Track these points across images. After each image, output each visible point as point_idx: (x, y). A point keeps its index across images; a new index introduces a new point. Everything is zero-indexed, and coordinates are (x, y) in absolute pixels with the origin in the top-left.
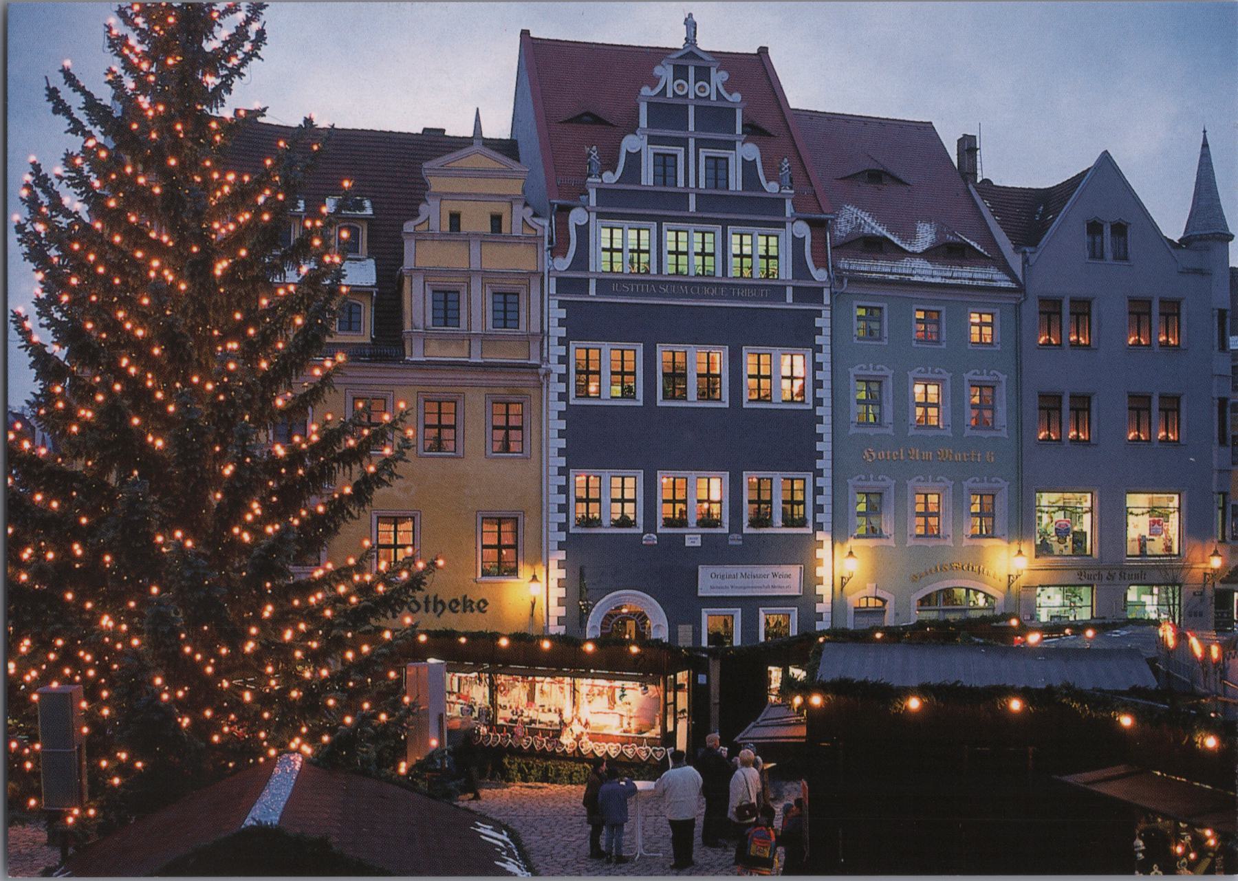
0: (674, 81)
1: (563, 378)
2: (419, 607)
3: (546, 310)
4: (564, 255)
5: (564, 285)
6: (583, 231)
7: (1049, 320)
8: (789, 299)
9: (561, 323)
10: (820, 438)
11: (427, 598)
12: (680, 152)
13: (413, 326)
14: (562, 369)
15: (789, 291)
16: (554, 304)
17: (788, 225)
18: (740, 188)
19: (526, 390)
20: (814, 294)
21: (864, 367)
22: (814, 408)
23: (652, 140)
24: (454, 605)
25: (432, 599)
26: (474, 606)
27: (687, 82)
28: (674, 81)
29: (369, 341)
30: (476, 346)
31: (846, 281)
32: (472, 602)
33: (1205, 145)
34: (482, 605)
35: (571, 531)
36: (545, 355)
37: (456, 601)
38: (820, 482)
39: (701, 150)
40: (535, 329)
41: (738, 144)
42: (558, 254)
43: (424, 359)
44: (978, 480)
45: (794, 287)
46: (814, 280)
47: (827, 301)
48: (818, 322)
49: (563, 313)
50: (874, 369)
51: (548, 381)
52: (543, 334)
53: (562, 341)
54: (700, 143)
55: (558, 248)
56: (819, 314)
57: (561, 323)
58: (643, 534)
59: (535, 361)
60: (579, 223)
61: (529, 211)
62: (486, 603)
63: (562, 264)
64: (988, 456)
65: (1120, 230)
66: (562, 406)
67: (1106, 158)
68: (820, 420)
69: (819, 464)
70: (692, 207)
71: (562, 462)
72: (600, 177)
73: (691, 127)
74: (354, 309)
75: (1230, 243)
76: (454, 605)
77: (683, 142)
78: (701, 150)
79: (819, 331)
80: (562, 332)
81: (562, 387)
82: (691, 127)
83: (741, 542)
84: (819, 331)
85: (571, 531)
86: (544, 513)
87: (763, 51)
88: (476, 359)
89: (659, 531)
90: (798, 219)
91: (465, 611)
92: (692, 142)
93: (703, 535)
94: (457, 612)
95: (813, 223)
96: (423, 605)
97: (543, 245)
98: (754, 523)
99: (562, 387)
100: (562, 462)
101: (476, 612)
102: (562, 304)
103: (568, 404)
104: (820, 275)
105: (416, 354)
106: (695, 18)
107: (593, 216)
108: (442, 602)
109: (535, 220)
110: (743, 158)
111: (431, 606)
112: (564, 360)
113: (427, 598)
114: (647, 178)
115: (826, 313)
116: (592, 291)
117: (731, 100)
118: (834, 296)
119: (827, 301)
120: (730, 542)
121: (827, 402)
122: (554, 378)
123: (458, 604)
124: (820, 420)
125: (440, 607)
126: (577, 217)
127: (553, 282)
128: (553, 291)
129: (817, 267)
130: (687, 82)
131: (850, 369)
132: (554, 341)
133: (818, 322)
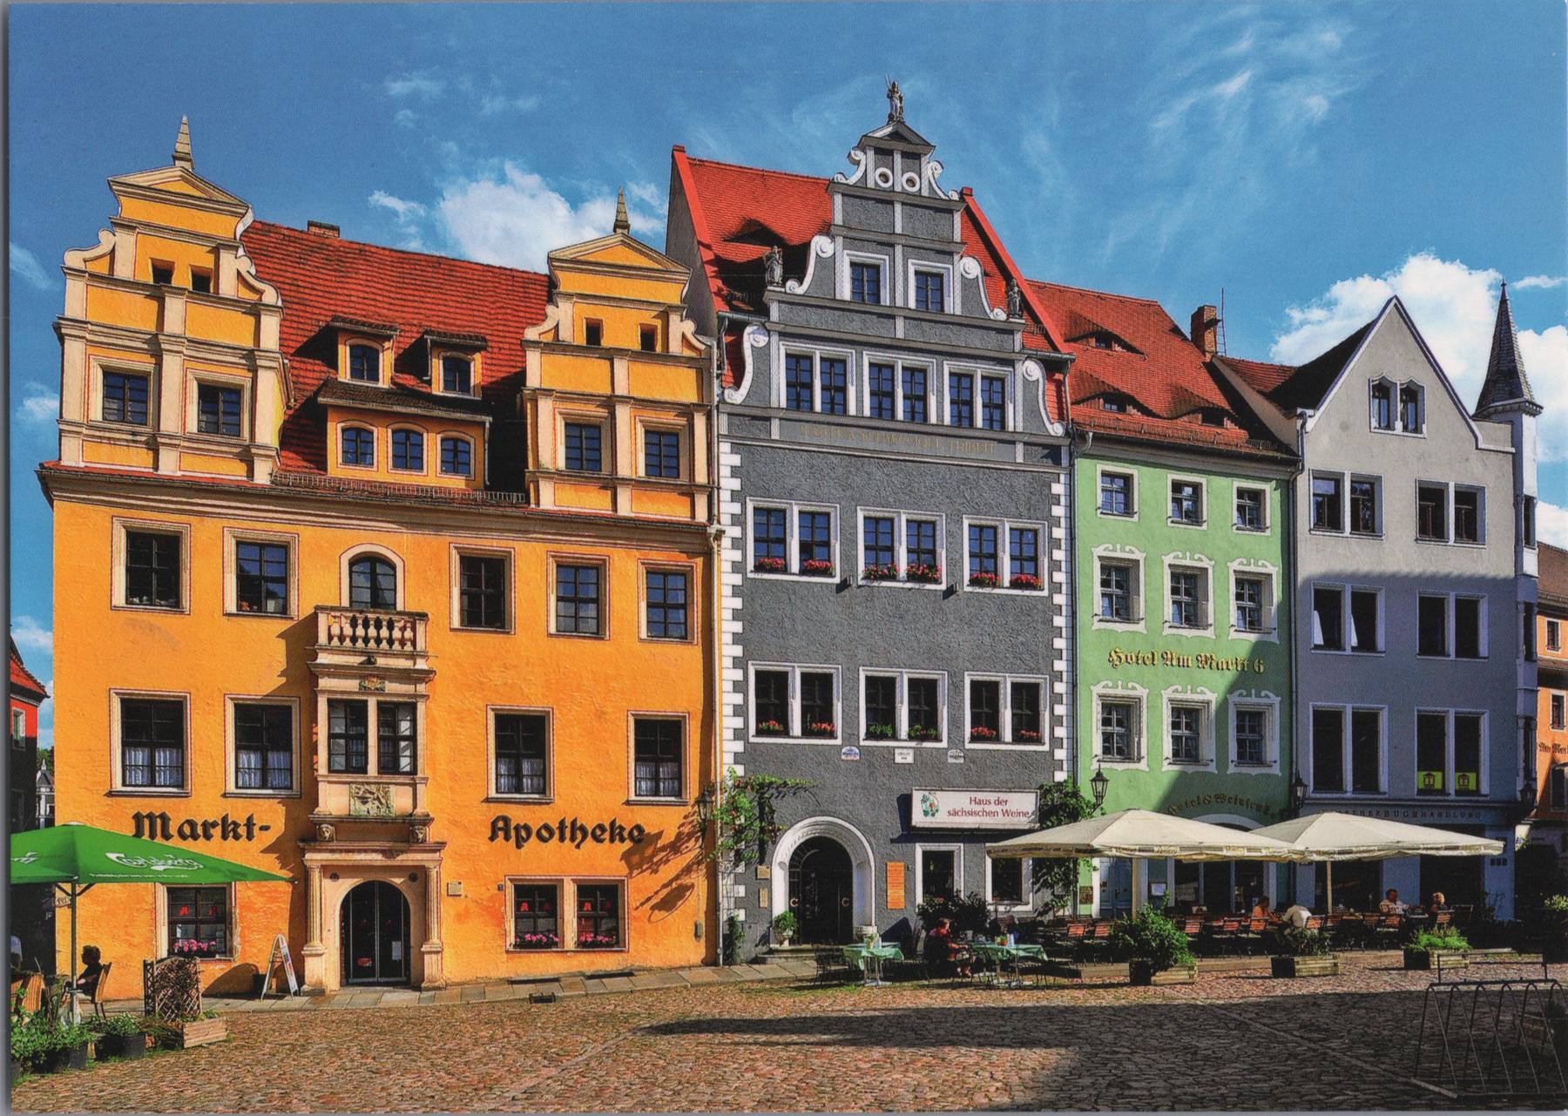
1: (738, 544)
4: (737, 384)
6: (762, 354)
9: (735, 472)
14: (736, 532)
21: (1111, 547)
43: (556, 508)
44: (1245, 693)
49: (736, 460)
50: (1123, 550)
51: (719, 546)
53: (736, 496)
57: (735, 472)
60: (756, 344)
63: (737, 397)
66: (737, 579)
71: (738, 651)
72: (784, 285)
80: (736, 484)
97: (710, 374)
100: (738, 651)
102: (735, 449)
103: (745, 578)
105: (549, 498)
107: (775, 338)
112: (738, 520)
114: (845, 291)
122: (726, 542)
126: (752, 338)
127: (724, 419)
128: (724, 431)
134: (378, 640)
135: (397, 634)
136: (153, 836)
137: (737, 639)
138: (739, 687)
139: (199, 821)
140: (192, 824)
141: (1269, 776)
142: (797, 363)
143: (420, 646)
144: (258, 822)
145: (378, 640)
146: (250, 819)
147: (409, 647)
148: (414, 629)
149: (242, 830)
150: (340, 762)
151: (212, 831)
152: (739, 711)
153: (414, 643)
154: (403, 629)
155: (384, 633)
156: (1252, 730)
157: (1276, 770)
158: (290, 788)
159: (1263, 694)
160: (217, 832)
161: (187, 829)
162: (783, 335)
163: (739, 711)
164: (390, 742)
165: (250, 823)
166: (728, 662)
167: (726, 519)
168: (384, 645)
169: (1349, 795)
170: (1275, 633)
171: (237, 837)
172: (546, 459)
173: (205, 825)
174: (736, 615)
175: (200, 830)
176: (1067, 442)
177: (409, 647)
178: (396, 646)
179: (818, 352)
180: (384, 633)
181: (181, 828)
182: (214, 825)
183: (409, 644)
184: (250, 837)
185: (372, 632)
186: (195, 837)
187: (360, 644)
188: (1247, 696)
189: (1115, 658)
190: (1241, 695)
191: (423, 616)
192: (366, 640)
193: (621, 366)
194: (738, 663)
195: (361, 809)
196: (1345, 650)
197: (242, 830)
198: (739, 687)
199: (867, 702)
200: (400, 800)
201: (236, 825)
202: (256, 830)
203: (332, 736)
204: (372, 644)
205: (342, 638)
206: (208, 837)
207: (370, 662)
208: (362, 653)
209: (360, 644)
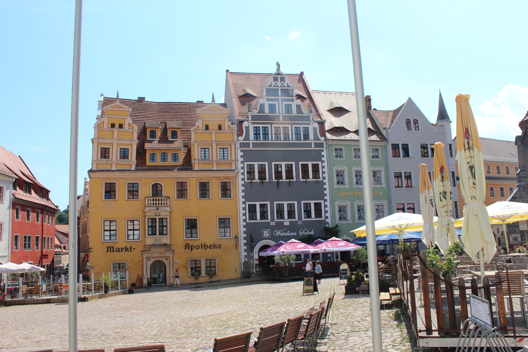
1: (243, 174)
2: (199, 247)
3: (236, 152)
5: (242, 145)
6: (247, 128)
7: (395, 150)
9: (242, 156)
10: (325, 189)
11: (202, 244)
12: (276, 103)
13: (195, 160)
14: (242, 171)
16: (239, 151)
17: (312, 124)
19: (231, 178)
20: (321, 145)
24: (210, 246)
25: (203, 245)
26: (217, 247)
29: (181, 165)
30: (215, 165)
32: (216, 245)
33: (440, 94)
34: (220, 246)
35: (248, 222)
36: (237, 167)
37: (211, 245)
39: (283, 102)
40: (233, 158)
41: (295, 100)
42: (240, 136)
48: (323, 153)
49: (242, 154)
52: (236, 160)
53: (242, 162)
55: (240, 134)
56: (323, 151)
57: (242, 156)
58: (271, 222)
59: (234, 168)
61: (230, 123)
62: (221, 246)
63: (241, 138)
64: (380, 193)
65: (416, 122)
66: (243, 182)
67: (410, 100)
68: (325, 184)
71: (244, 200)
74: (176, 155)
75: (451, 124)
76: (210, 246)
77: (277, 100)
78: (283, 102)
79: (323, 156)
80: (242, 159)
81: (243, 177)
83: (302, 224)
84: (323, 156)
85: (248, 222)
86: (238, 216)
87: (302, 73)
88: (215, 168)
89: (276, 221)
91: (214, 248)
94: (211, 248)
96: (201, 247)
99: (243, 177)
100: (244, 200)
101: (218, 248)
102: (241, 151)
103: (245, 182)
106: (279, 63)
107: (250, 123)
108: (206, 245)
109: (232, 125)
111: (203, 247)
112: (243, 168)
113: (202, 244)
115: (325, 151)
116: (251, 146)
118: (327, 145)
119: (325, 146)
120: (299, 224)
122: (240, 174)
123: (212, 246)
124: (325, 184)
125: (206, 247)
126: (245, 124)
128: (239, 146)
129: (321, 137)
130: (278, 81)
131: (333, 168)
132: (239, 162)
133: (323, 153)
134: (159, 204)
135: (163, 202)
136: (111, 251)
137: (243, 197)
138: (244, 209)
139: (120, 248)
140: (119, 248)
142: (256, 129)
143: (168, 205)
144: (133, 248)
145: (159, 204)
146: (131, 247)
147: (165, 205)
148: (167, 201)
149: (129, 250)
150: (150, 233)
151: (123, 250)
152: (244, 215)
153: (167, 204)
154: (164, 201)
155: (160, 202)
158: (139, 239)
160: (124, 250)
161: (117, 250)
162: (252, 123)
163: (244, 215)
164: (162, 227)
165: (131, 248)
166: (241, 203)
167: (240, 168)
168: (160, 205)
170: (384, 185)
171: (128, 251)
172: (196, 157)
173: (121, 248)
174: (243, 191)
175: (120, 250)
176: (325, 141)
177: (165, 205)
178: (163, 205)
179: (261, 126)
180: (160, 202)
181: (116, 250)
182: (123, 248)
183: (165, 204)
184: (131, 251)
185: (157, 202)
186: (119, 251)
187: (155, 205)
191: (169, 197)
192: (156, 204)
193: (214, 135)
194: (244, 203)
195: (156, 243)
197: (129, 250)
198: (244, 209)
200: (165, 240)
201: (128, 248)
202: (132, 249)
203: (149, 227)
204: (157, 205)
205: (151, 204)
206: (122, 251)
207: (157, 209)
208: (155, 206)
209: (155, 205)
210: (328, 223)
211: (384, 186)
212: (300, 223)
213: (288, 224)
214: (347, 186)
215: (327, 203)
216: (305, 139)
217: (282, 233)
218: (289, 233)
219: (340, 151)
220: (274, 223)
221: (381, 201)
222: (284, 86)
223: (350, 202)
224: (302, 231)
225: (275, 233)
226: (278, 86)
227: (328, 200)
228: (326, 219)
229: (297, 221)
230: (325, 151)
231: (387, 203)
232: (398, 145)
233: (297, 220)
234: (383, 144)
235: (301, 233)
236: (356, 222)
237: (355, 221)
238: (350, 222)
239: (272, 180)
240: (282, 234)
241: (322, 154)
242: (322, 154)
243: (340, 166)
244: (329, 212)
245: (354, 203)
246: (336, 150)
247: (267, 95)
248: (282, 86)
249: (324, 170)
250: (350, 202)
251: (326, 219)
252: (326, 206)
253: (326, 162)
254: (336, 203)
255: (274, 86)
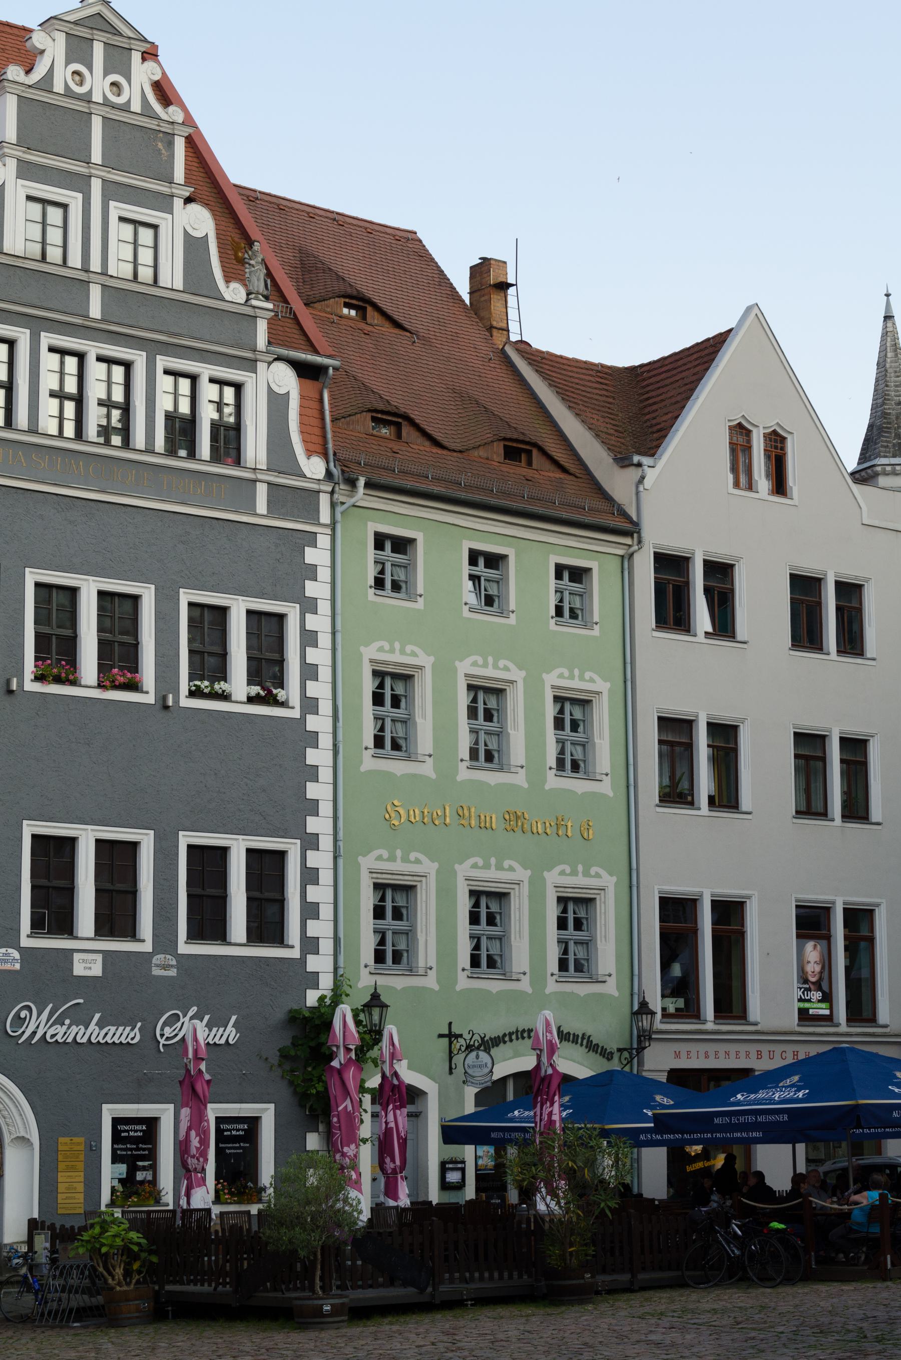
0: (67, 63)
8: (262, 506)
10: (313, 773)
12: (74, 200)
15: (262, 491)
17: (261, 366)
18: (179, 284)
22: (303, 720)
23: (26, 171)
27: (90, 69)
28: (67, 63)
31: (362, 482)
33: (888, 318)
38: (314, 859)
39: (112, 204)
41: (178, 203)
44: (568, 870)
45: (269, 484)
46: (305, 476)
47: (325, 516)
48: (311, 556)
54: (112, 191)
68: (313, 739)
69: (313, 825)
70: (95, 311)
73: (96, 156)
77: (81, 183)
78: (112, 204)
79: (312, 572)
82: (96, 156)
83: (173, 973)
84: (312, 572)
89: (25, 942)
90: (279, 359)
92: (96, 186)
93: (106, 954)
95: (305, 371)
98: (196, 933)
104: (314, 468)
110: (185, 232)
115: (324, 541)
117: (164, 116)
118: (339, 509)
119: (325, 516)
120: (156, 972)
121: (325, 707)
124: (313, 739)
129: (309, 453)
130: (90, 69)
131: (362, 649)
133: (311, 556)
141: (601, 995)
156: (578, 925)
157: (611, 988)
159: (594, 870)
169: (710, 1026)
170: (607, 780)
188: (571, 874)
189: (393, 815)
190: (562, 873)
196: (699, 809)
199: (33, 875)
210: (313, 980)
211: (605, 787)
212: (165, 967)
213: (96, 970)
214: (427, 769)
215: (320, 859)
216: (216, 456)
217: (60, 1022)
218: (101, 1025)
219: (399, 558)
220: (16, 955)
221: (589, 876)
222: (125, 108)
223: (436, 865)
224: (176, 1017)
225: (19, 1021)
226: (87, 98)
227: (326, 842)
228: (310, 957)
229: (145, 958)
230: (324, 541)
231: (616, 884)
232: (686, 560)
233: (147, 947)
234: (614, 546)
235: (168, 1031)
236: (458, 988)
237: (455, 981)
238: (431, 982)
239: (21, 684)
240: (61, 1030)
241: (308, 560)
242: (308, 560)
243: (397, 645)
244: (326, 911)
245: (455, 872)
246: (380, 541)
247: (23, 142)
248: (114, 99)
249: (313, 655)
250: (436, 865)
251: (310, 957)
252: (310, 876)
253: (324, 607)
254: (367, 862)
255: (69, 93)
